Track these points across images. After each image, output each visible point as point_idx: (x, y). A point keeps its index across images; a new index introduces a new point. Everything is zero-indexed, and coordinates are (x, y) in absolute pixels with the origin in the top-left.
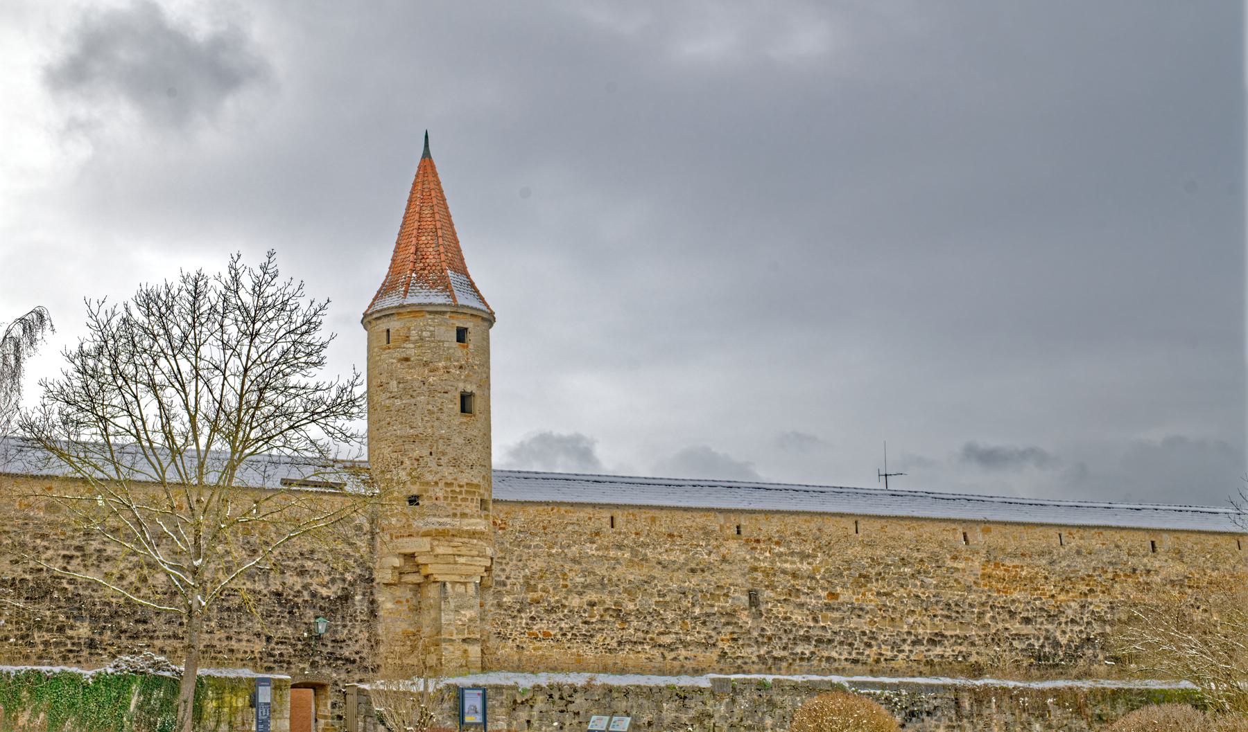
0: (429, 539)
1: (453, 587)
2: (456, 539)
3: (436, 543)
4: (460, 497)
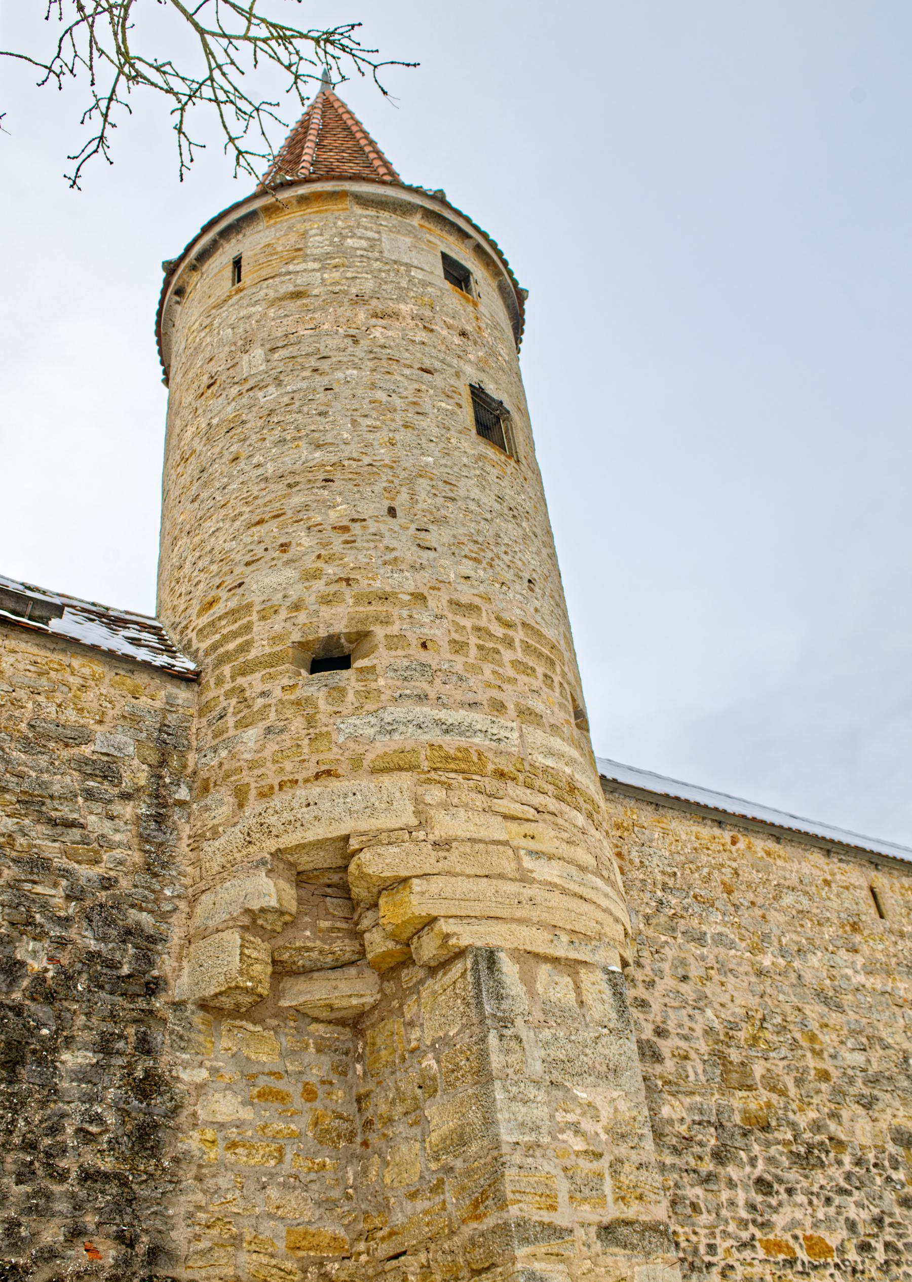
0: (406, 779)
1: (528, 981)
2: (512, 789)
3: (435, 794)
4: (507, 655)
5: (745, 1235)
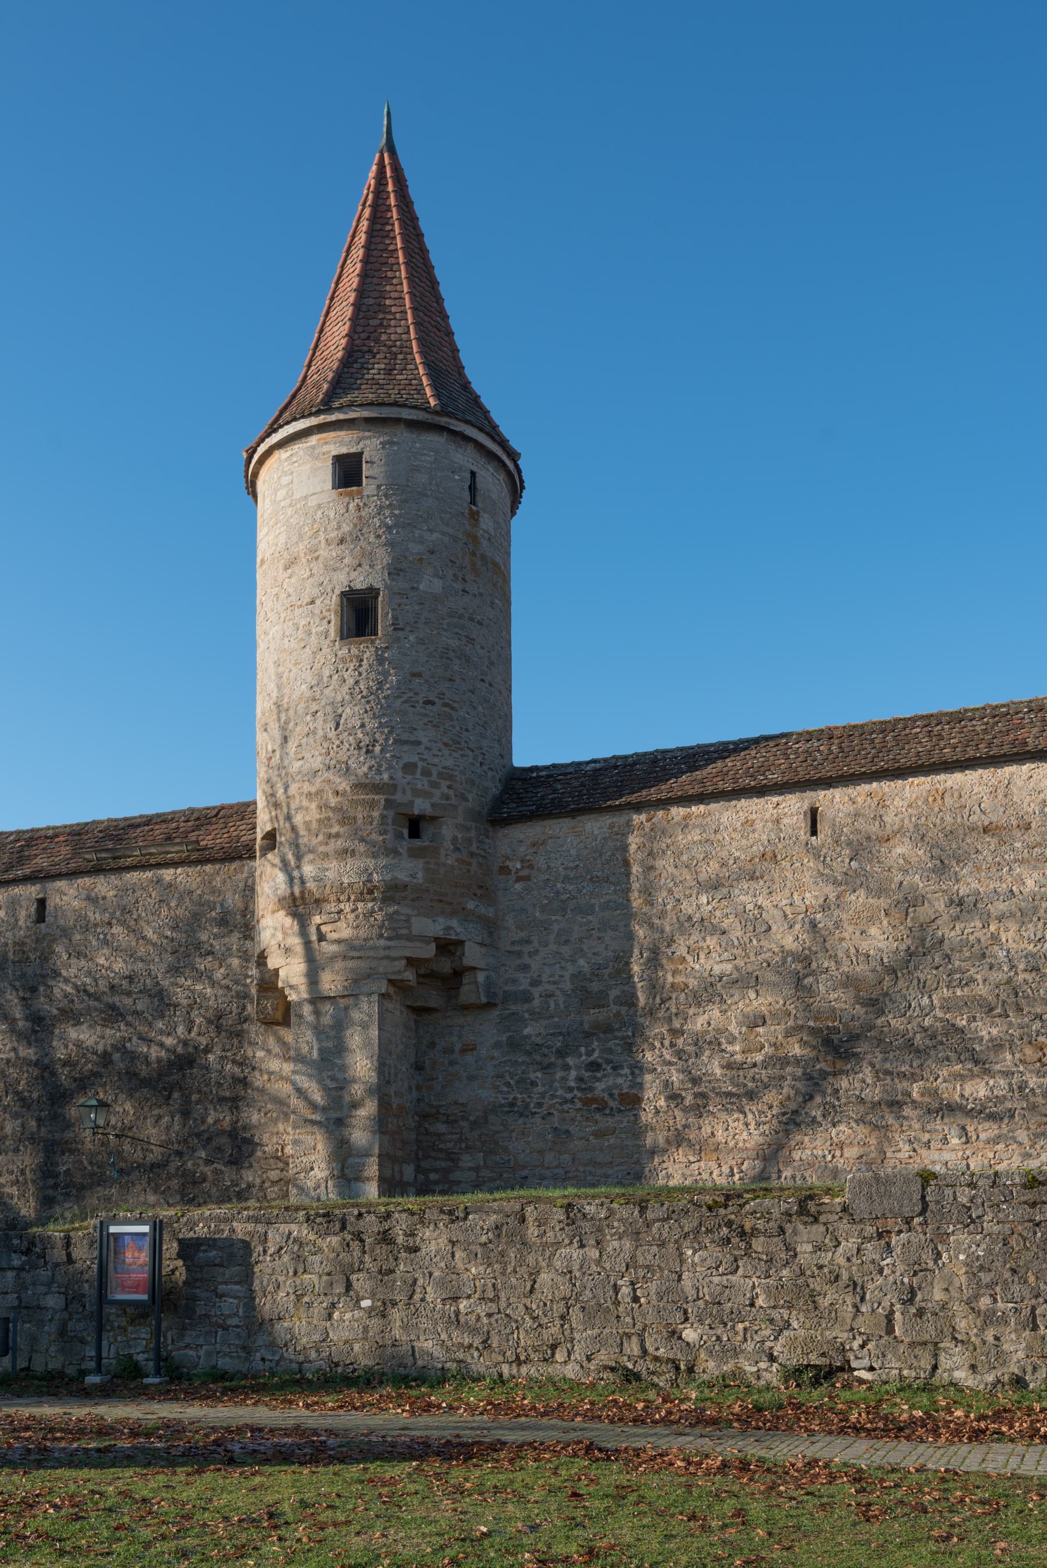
5: (569, 1096)
